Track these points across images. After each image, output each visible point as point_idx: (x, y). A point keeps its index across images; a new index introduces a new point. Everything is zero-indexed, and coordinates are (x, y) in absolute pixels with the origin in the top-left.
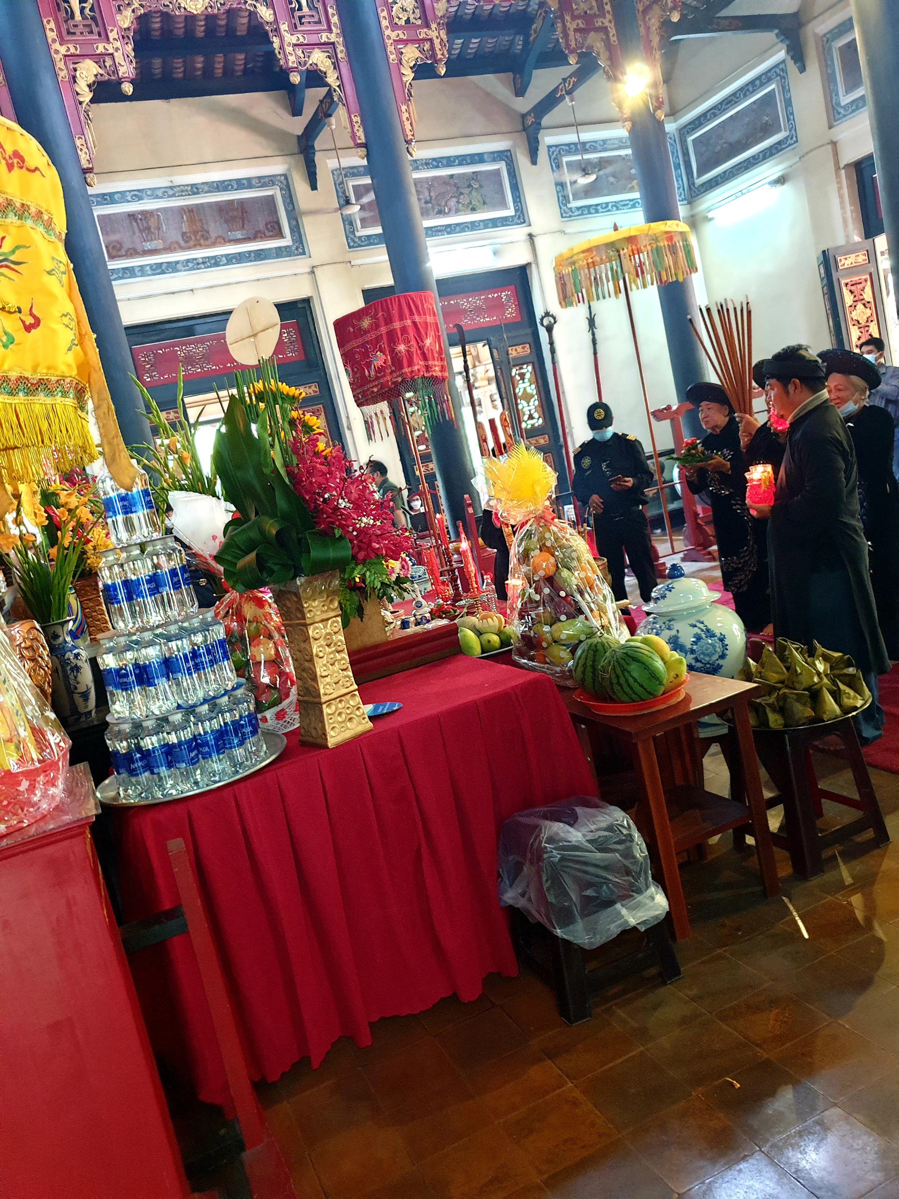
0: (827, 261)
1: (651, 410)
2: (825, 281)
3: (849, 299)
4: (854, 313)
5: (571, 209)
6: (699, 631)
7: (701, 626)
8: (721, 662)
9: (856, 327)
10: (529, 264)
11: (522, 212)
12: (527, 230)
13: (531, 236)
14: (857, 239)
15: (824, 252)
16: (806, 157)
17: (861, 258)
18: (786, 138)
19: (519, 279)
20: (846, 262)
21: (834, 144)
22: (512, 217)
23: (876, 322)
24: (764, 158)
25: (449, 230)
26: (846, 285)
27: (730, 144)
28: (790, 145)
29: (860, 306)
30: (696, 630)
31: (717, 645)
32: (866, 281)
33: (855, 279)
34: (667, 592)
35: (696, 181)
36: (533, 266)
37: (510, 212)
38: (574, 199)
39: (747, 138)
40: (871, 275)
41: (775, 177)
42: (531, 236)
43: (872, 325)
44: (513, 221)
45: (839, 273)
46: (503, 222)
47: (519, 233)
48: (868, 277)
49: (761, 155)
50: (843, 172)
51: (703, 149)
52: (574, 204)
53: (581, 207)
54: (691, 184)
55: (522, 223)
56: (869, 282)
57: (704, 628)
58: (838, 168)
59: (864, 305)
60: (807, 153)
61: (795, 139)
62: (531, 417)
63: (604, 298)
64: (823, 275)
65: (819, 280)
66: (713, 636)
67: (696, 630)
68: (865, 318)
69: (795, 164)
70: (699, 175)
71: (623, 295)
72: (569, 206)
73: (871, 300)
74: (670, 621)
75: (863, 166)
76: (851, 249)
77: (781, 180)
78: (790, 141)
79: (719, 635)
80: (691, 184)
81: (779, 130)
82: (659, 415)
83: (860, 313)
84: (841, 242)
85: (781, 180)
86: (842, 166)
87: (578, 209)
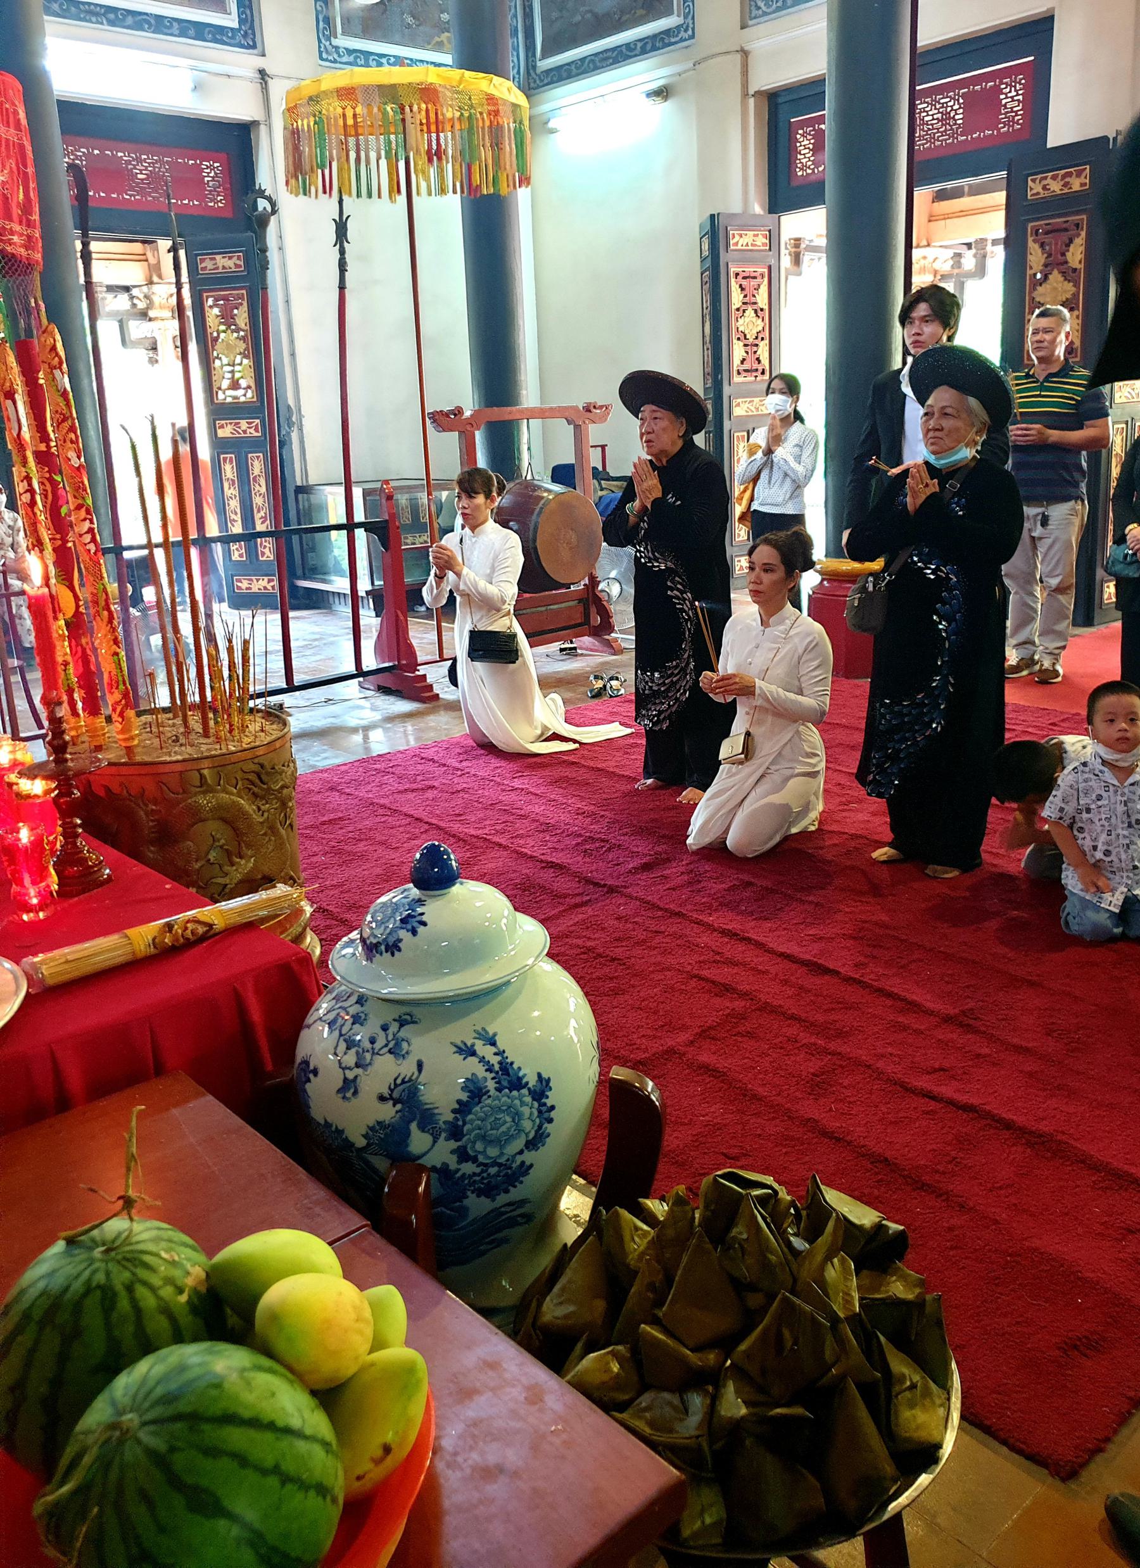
0: (715, 232)
1: (429, 409)
2: (708, 264)
3: (737, 298)
4: (741, 321)
5: (337, 48)
6: (480, 1071)
7: (487, 1051)
8: (529, 1157)
9: (741, 344)
10: (255, 123)
11: (252, 27)
12: (260, 62)
13: (262, 73)
14: (758, 209)
15: (712, 216)
16: (703, 65)
17: (761, 241)
18: (678, 27)
19: (235, 142)
20: (741, 240)
21: (745, 53)
22: (232, 29)
23: (767, 341)
24: (644, 51)
25: (112, 16)
26: (737, 275)
27: (595, 16)
28: (682, 40)
29: (750, 312)
30: (473, 1066)
31: (526, 1110)
32: (762, 276)
33: (749, 270)
34: (403, 934)
35: (539, 64)
36: (263, 128)
37: (230, 21)
38: (343, 33)
39: (622, 12)
40: (770, 267)
41: (655, 85)
42: (262, 73)
43: (762, 344)
44: (233, 38)
45: (730, 255)
46: (217, 35)
47: (243, 62)
48: (766, 270)
49: (639, 45)
50: (752, 101)
51: (555, 15)
52: (343, 42)
53: (355, 51)
54: (531, 66)
55: (249, 47)
56: (766, 279)
57: (495, 1060)
58: (745, 95)
59: (756, 312)
60: (705, 59)
61: (690, 32)
62: (235, 385)
63: (370, 196)
64: (706, 253)
65: (699, 260)
66: (517, 1084)
67: (473, 1066)
68: (754, 332)
69: (685, 72)
70: (544, 56)
71: (402, 199)
72: (335, 42)
73: (766, 307)
74: (402, 1023)
75: (780, 100)
76: (747, 223)
77: (662, 93)
78: (682, 34)
79: (532, 1080)
80: (531, 66)
81: (669, 12)
82: (445, 420)
83: (749, 324)
84: (736, 207)
85: (662, 93)
86: (751, 92)
87: (350, 52)
